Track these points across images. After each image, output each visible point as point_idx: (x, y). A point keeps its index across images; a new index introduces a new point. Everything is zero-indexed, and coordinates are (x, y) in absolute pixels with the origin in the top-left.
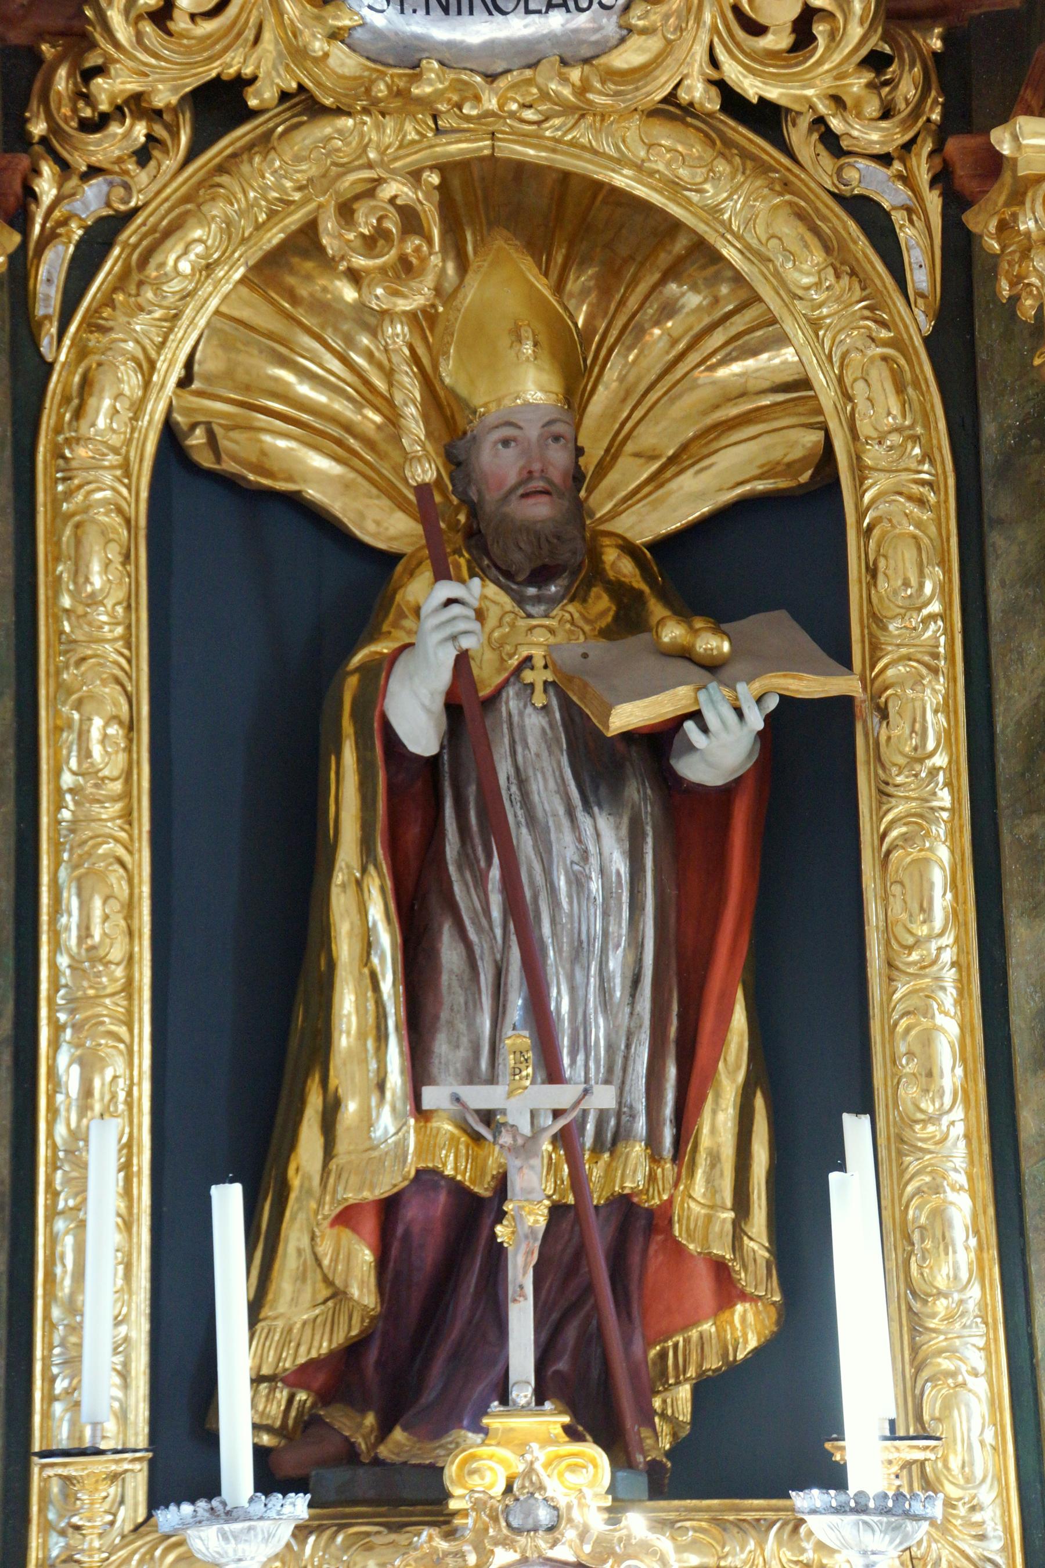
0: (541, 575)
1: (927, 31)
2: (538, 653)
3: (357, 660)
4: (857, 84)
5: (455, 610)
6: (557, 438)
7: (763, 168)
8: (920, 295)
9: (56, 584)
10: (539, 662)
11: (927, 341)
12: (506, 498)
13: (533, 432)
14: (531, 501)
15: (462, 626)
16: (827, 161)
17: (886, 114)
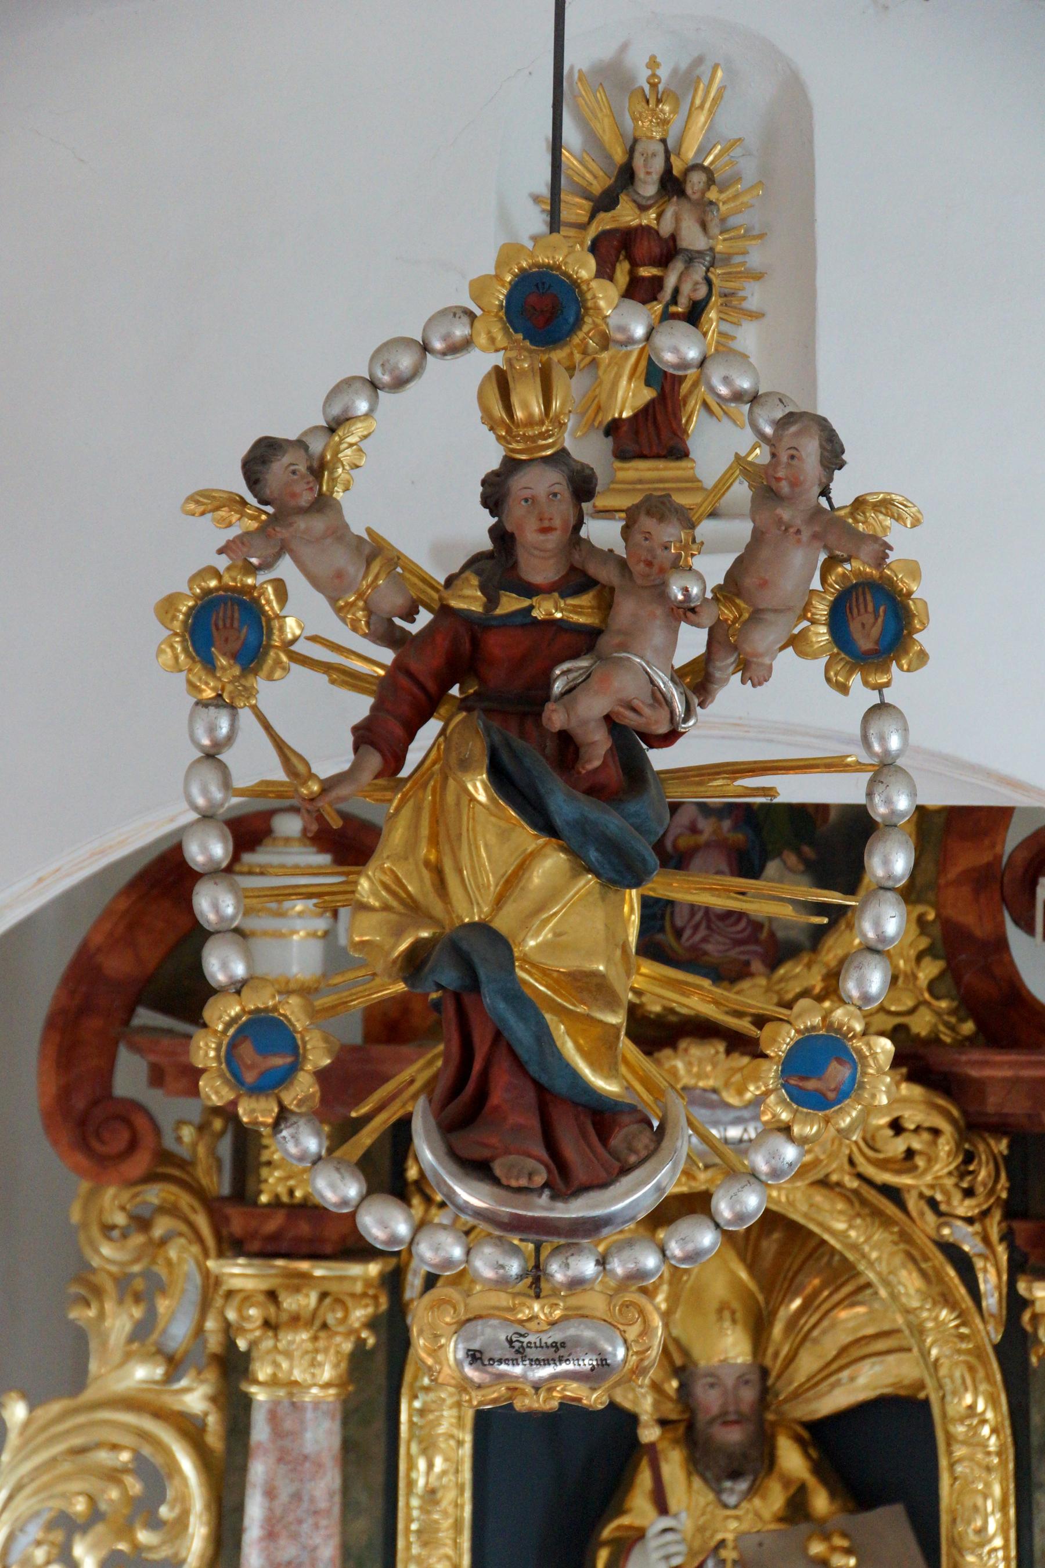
0: (735, 1475)
1: (998, 1140)
2: (730, 1537)
3: (606, 1533)
4: (949, 1182)
5: (669, 1537)
6: (747, 1382)
7: (887, 1222)
8: (992, 1315)
9: (412, 1466)
10: (730, 1544)
11: (997, 1348)
12: (712, 1421)
13: (730, 1382)
14: (729, 1429)
15: (673, 1549)
16: (930, 1218)
17: (969, 1193)
